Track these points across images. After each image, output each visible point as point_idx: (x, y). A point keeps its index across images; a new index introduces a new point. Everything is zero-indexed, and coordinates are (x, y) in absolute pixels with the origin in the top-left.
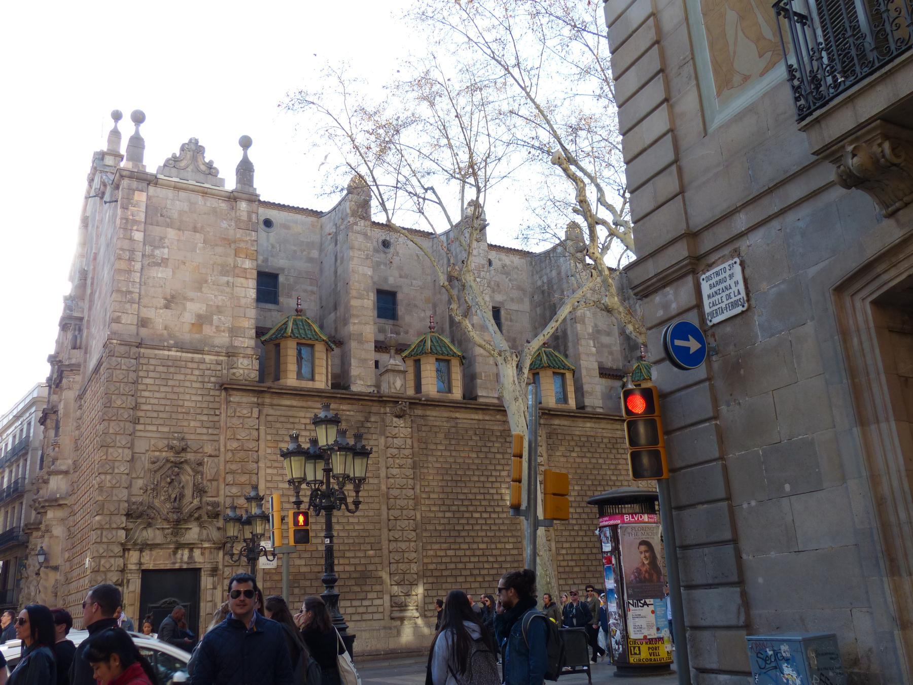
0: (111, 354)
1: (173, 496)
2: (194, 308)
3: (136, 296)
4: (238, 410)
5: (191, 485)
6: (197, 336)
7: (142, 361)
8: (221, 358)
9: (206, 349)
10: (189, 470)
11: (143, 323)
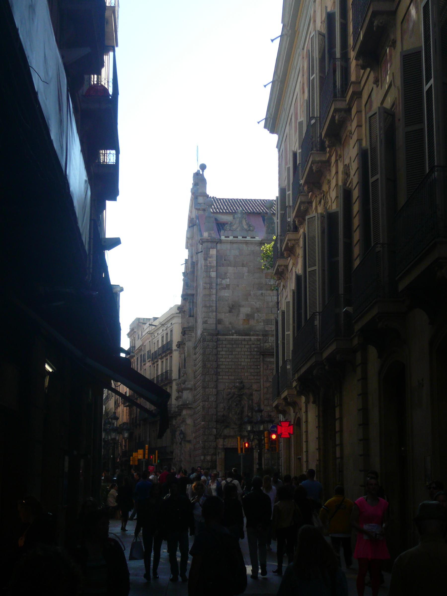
0: (204, 340)
1: (238, 412)
2: (245, 310)
3: (214, 308)
4: (269, 365)
5: (247, 405)
6: (247, 326)
7: (219, 343)
8: (260, 337)
9: (252, 333)
10: (246, 398)
11: (219, 322)
